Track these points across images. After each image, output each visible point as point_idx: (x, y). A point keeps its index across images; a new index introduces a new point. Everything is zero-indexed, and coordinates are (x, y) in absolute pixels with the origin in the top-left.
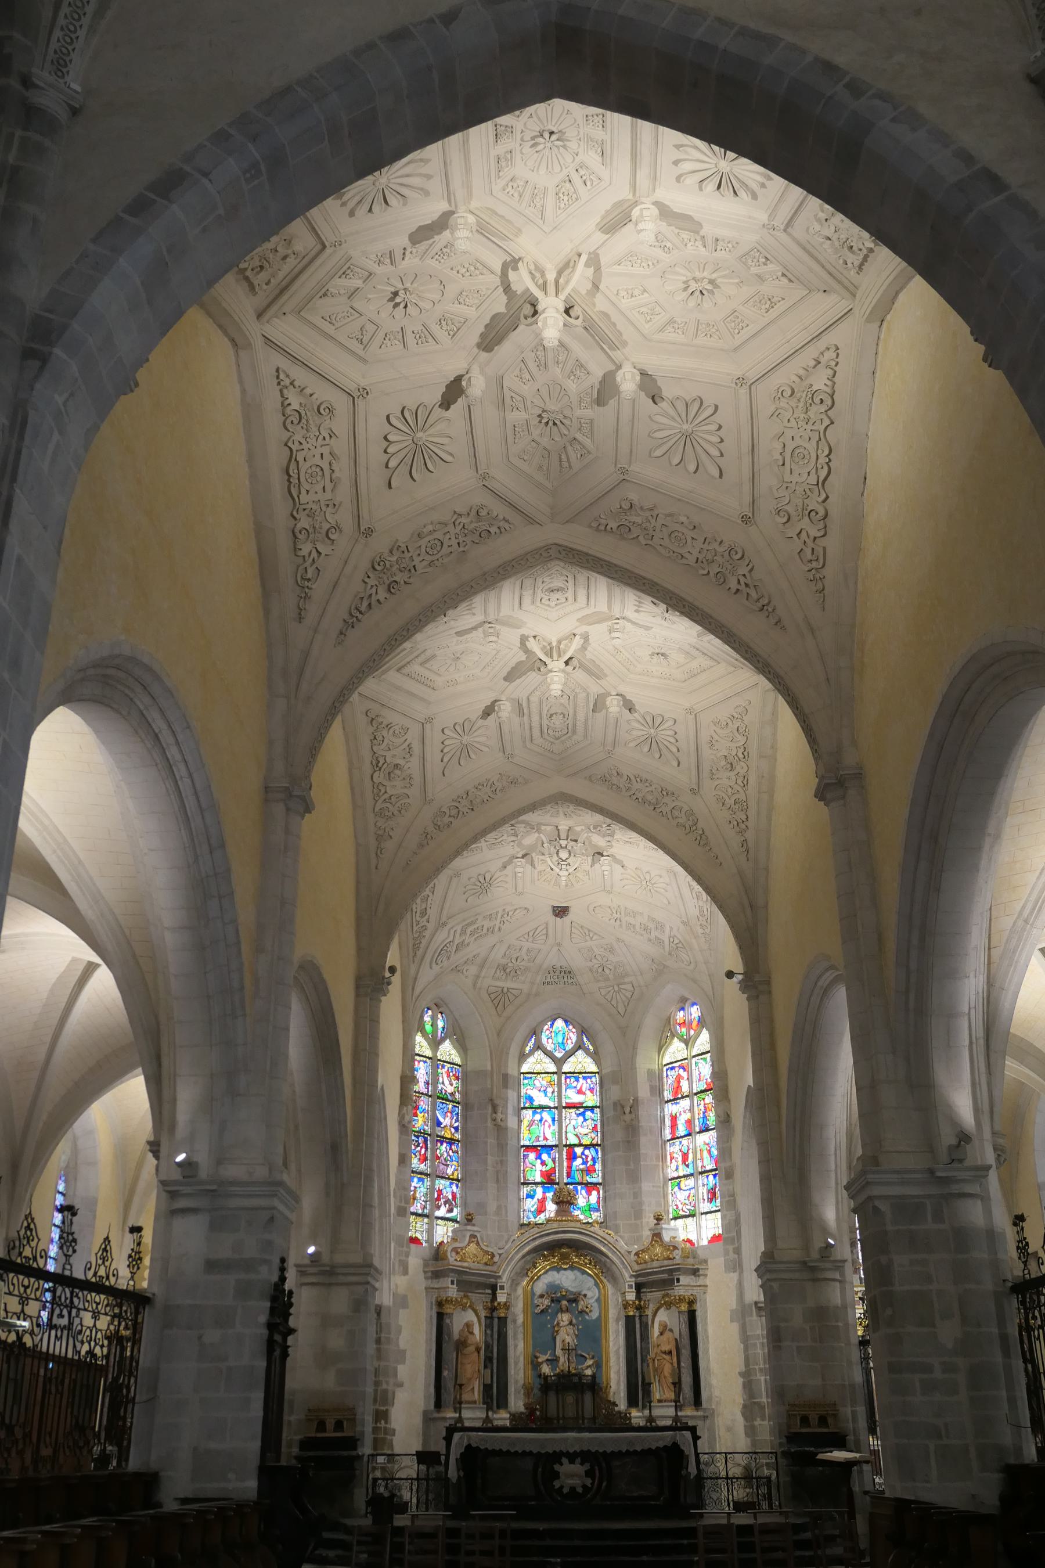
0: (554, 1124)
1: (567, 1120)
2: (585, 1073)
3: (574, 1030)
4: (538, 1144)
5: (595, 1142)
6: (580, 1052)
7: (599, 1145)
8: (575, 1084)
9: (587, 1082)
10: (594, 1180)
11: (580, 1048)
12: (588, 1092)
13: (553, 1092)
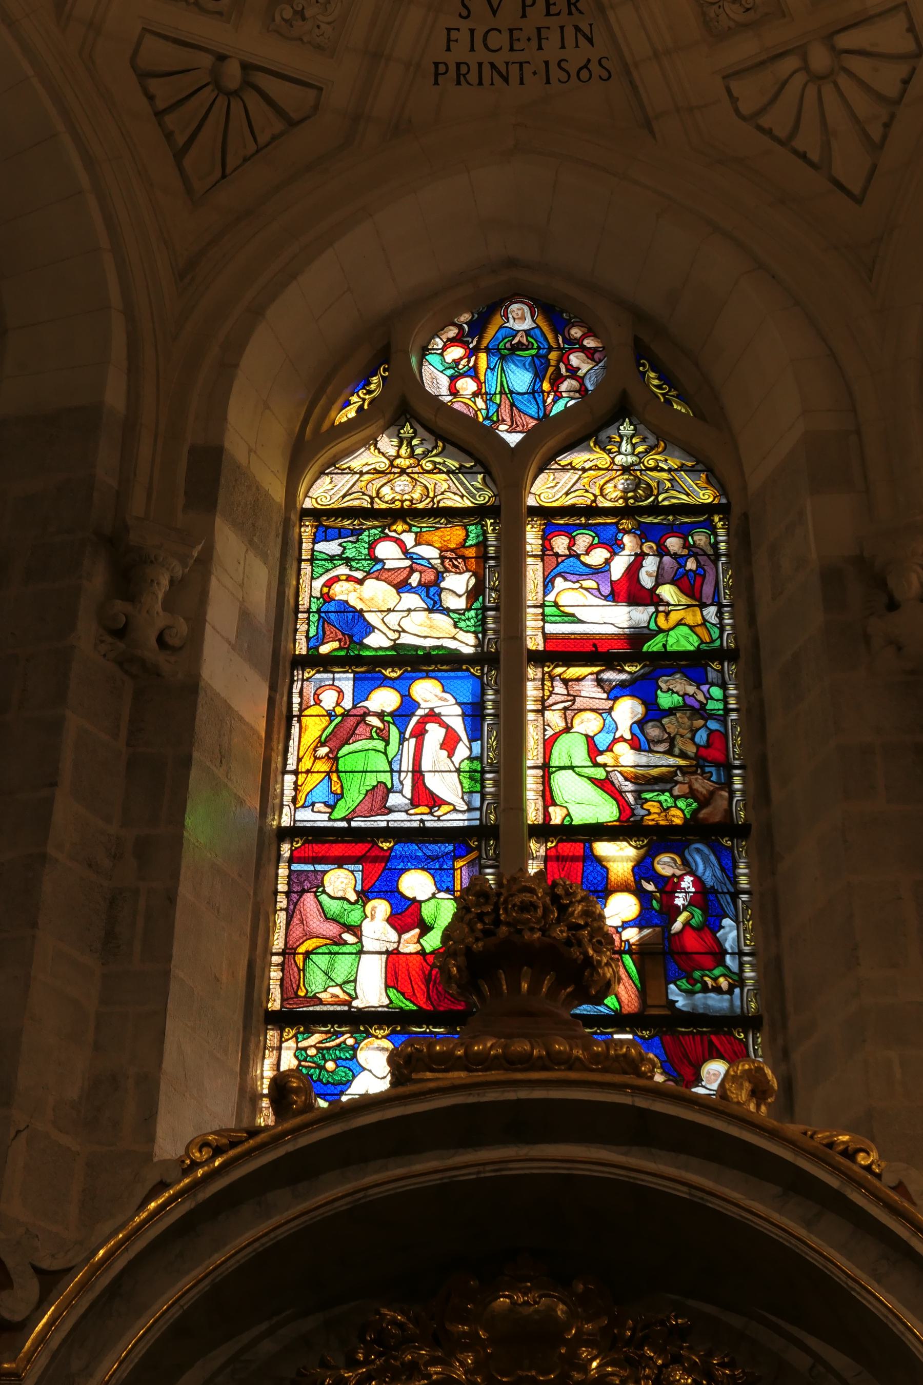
0: (475, 734)
1: (555, 719)
2: (655, 509)
3: (589, 343)
4: (380, 822)
5: (713, 813)
6: (626, 429)
7: (741, 832)
8: (598, 556)
9: (662, 552)
10: (717, 1003)
11: (621, 412)
12: (668, 592)
13: (473, 594)
